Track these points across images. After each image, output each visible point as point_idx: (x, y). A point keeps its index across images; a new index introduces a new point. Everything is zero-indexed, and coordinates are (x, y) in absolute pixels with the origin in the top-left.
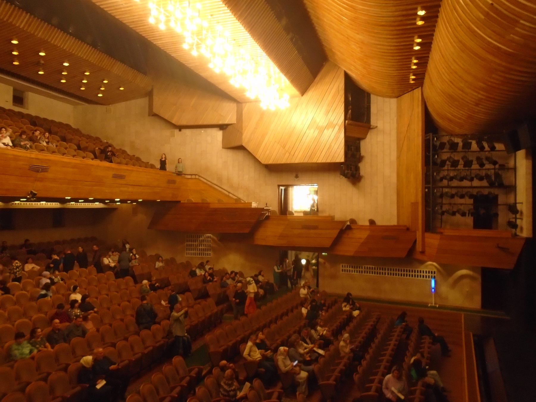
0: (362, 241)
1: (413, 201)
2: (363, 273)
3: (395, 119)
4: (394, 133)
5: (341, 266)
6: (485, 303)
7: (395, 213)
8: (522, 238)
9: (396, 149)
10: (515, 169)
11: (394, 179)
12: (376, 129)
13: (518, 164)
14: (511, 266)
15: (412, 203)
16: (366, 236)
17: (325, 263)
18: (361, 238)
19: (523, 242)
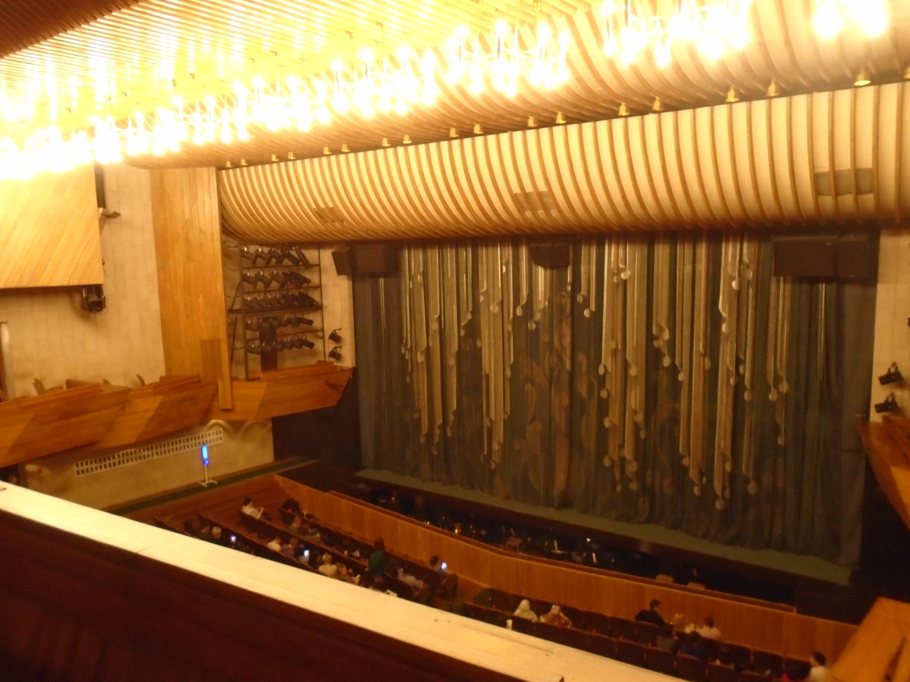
0: (150, 414)
1: (205, 336)
2: (117, 466)
3: (150, 204)
4: (149, 227)
5: (75, 466)
6: (279, 452)
7: (160, 355)
8: (349, 370)
9: (154, 255)
10: (319, 287)
11: (155, 303)
12: (118, 219)
13: (324, 282)
14: (334, 403)
15: (203, 343)
16: (156, 405)
17: (40, 471)
18: (148, 411)
19: (349, 375)
